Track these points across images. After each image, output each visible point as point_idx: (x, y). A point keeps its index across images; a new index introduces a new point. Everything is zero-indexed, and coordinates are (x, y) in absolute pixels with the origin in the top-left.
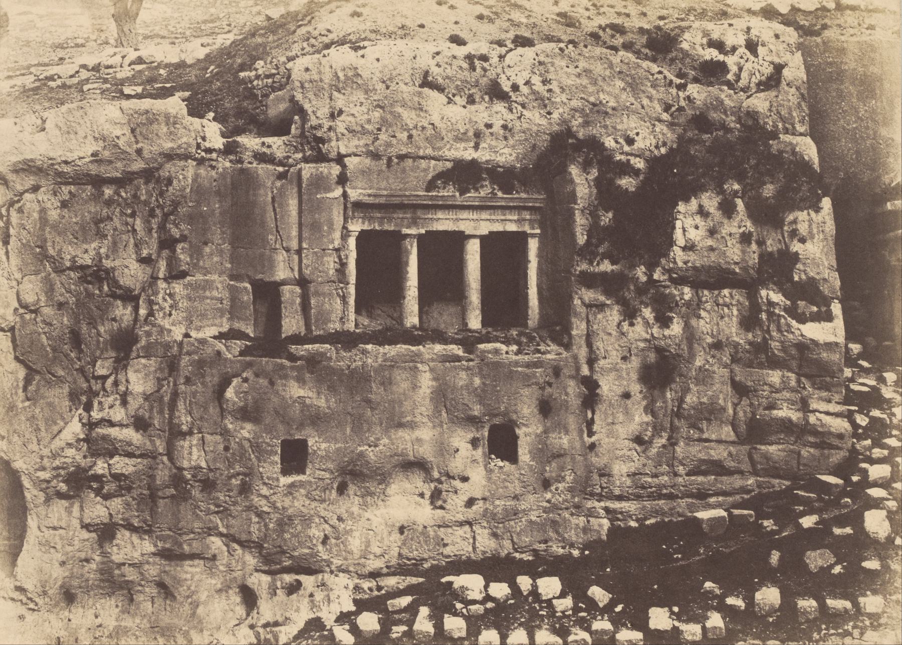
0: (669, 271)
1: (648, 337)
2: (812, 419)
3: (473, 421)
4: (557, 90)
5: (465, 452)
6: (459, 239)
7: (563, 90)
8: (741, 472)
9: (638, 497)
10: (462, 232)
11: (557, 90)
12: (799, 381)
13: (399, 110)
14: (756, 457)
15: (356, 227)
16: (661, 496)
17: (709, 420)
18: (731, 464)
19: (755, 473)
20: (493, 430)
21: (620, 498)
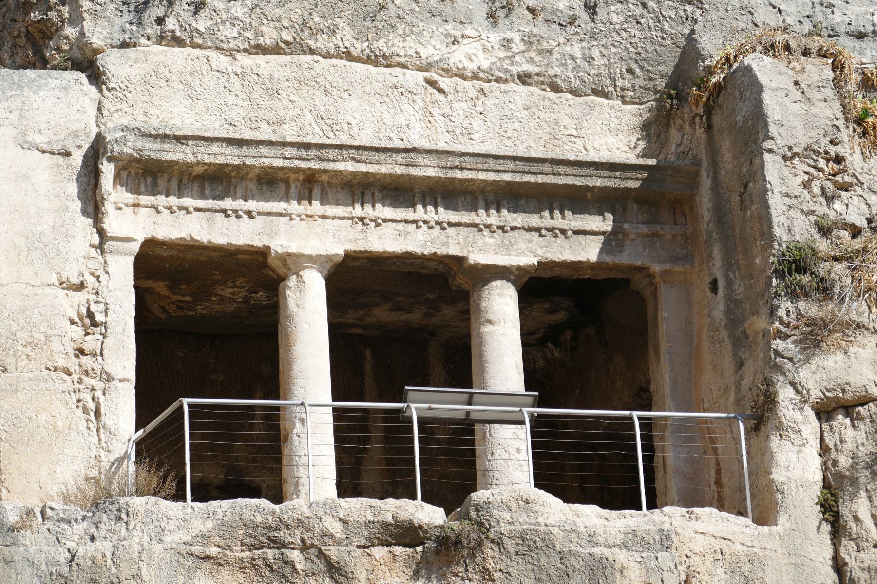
6: (448, 286)
10: (460, 260)
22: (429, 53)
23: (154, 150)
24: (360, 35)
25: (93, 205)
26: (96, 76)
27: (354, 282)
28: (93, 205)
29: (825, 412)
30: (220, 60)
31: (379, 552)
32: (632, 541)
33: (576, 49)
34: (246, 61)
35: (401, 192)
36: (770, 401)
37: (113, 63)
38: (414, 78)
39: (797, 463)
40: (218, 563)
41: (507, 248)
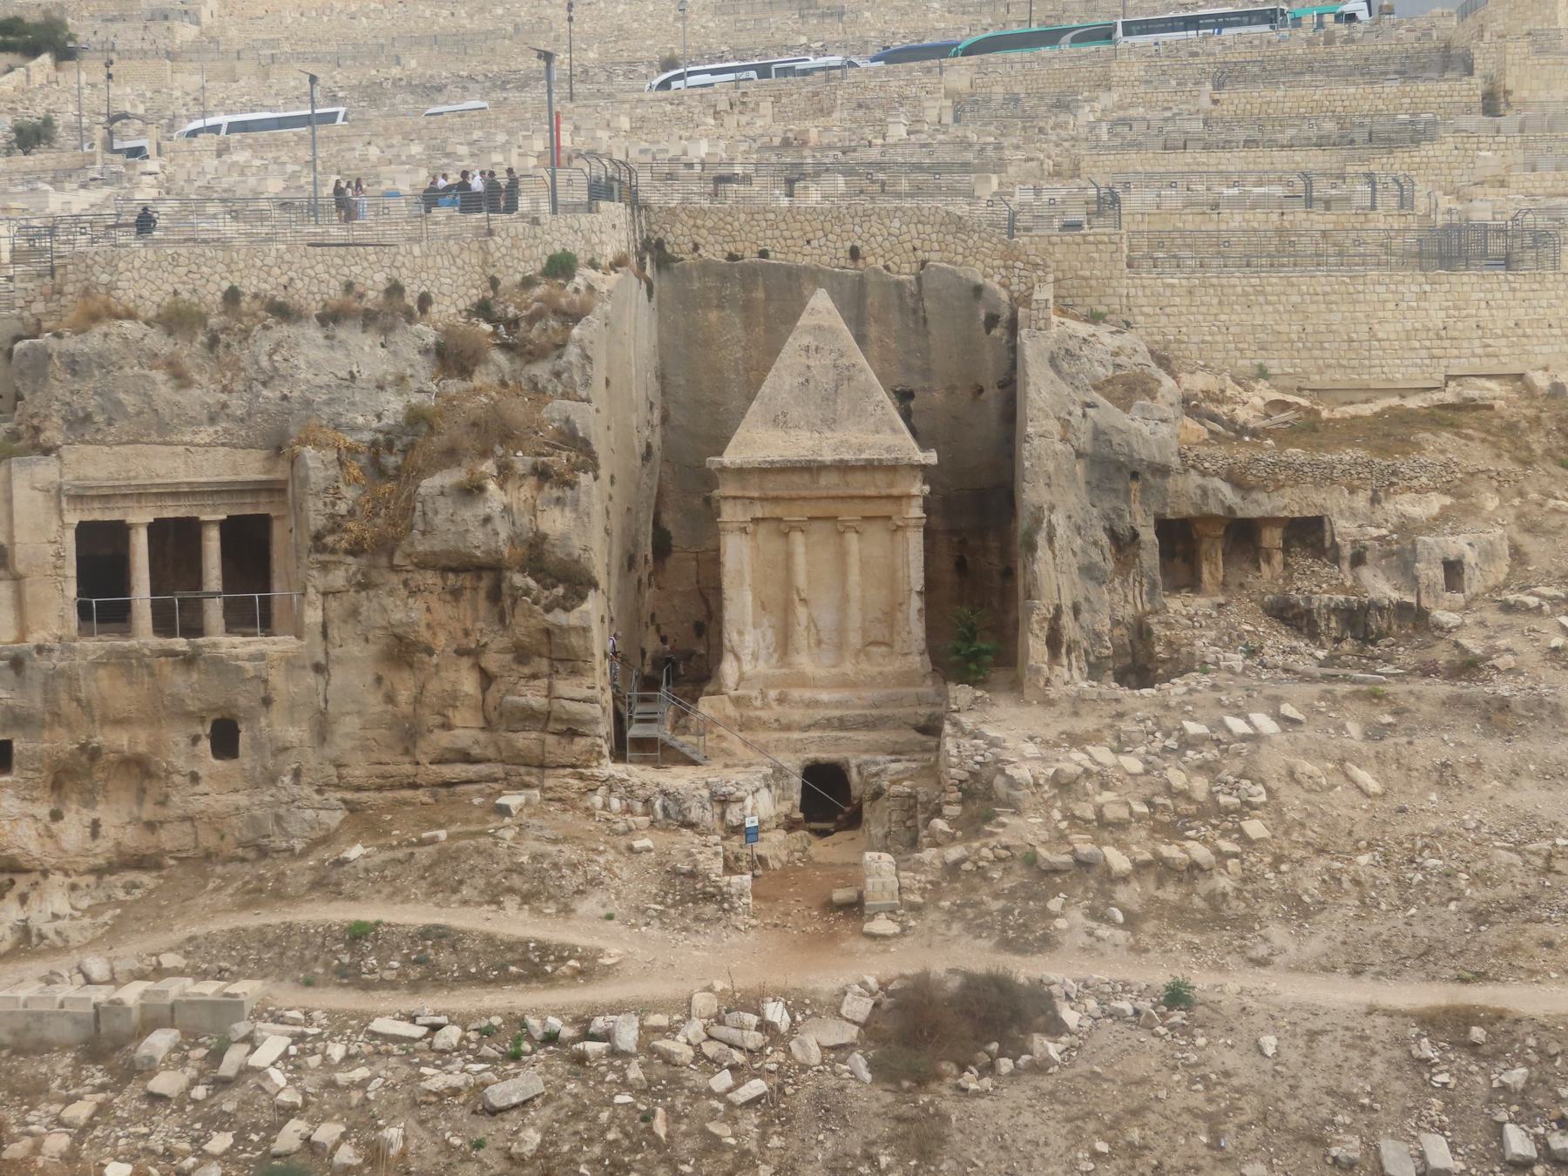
0: (409, 555)
1: (385, 623)
2: (556, 704)
3: (189, 716)
4: (303, 365)
5: (184, 750)
7: (309, 364)
8: (489, 760)
9: (380, 788)
11: (303, 365)
12: (551, 666)
13: (122, 396)
14: (502, 745)
15: (73, 518)
16: (402, 787)
17: (455, 707)
18: (476, 751)
19: (503, 761)
20: (217, 724)
21: (359, 789)
22: (187, 438)
23: (81, 492)
24: (160, 435)
25: (61, 513)
26: (59, 457)
27: (158, 530)
28: (61, 513)
29: (325, 594)
30: (106, 449)
31: (162, 659)
32: (252, 658)
33: (243, 433)
34: (116, 448)
35: (176, 495)
36: (305, 588)
37: (64, 450)
38: (181, 449)
39: (313, 616)
40: (105, 664)
41: (214, 512)
